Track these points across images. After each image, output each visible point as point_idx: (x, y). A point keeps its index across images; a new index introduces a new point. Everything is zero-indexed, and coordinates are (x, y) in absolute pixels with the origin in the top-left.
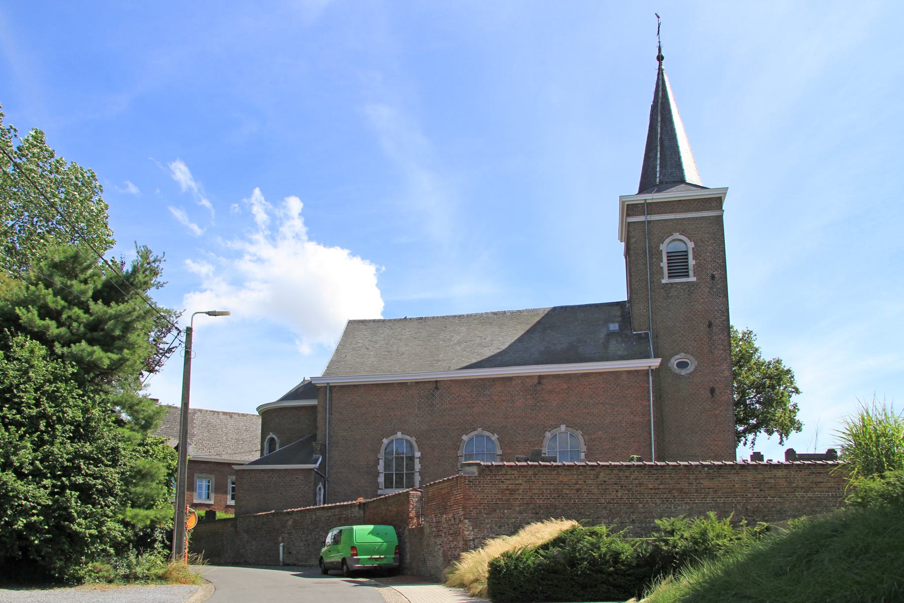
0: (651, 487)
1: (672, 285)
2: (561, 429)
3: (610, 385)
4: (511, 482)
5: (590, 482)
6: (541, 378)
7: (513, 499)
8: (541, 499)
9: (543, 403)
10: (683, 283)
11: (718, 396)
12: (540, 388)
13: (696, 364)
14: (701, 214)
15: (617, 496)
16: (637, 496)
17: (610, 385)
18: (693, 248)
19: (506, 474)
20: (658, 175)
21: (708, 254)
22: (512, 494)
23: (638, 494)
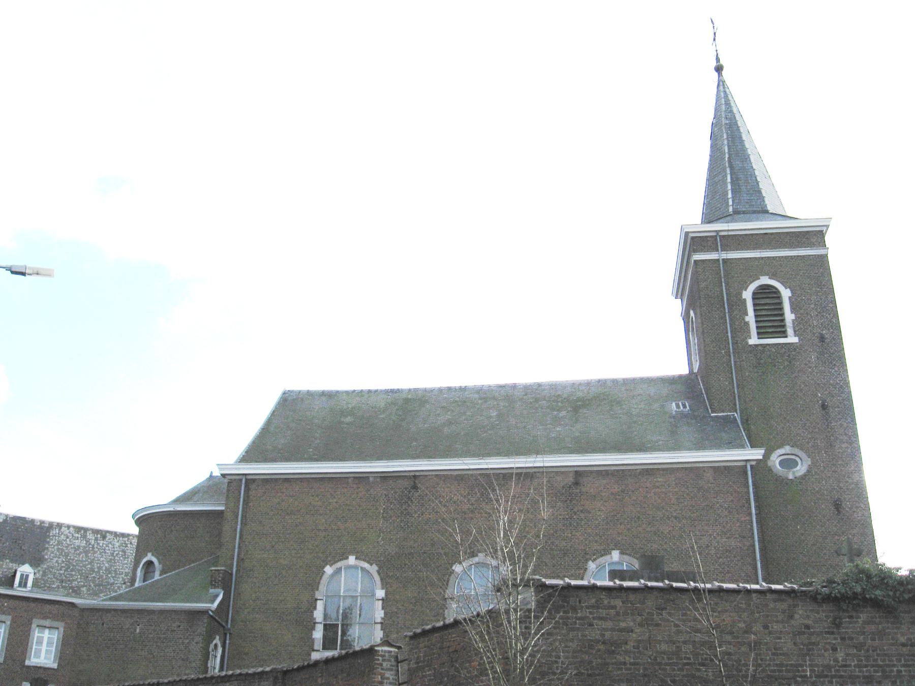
0: (902, 639)
1: (764, 347)
2: (612, 558)
3: (687, 488)
4: (609, 624)
5: (776, 627)
6: (579, 474)
7: (615, 663)
8: (676, 664)
9: (582, 515)
10: (780, 344)
11: (847, 511)
12: (578, 491)
13: (810, 463)
14: (797, 252)
15: (836, 660)
16: (876, 660)
17: (687, 488)
18: (790, 298)
19: (598, 608)
20: (730, 203)
21: (812, 306)
22: (613, 651)
23: (878, 655)
